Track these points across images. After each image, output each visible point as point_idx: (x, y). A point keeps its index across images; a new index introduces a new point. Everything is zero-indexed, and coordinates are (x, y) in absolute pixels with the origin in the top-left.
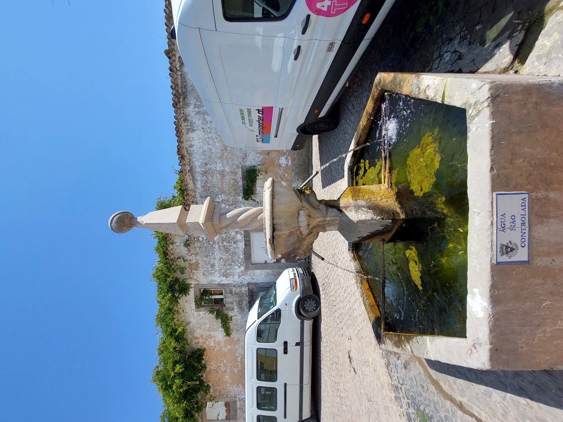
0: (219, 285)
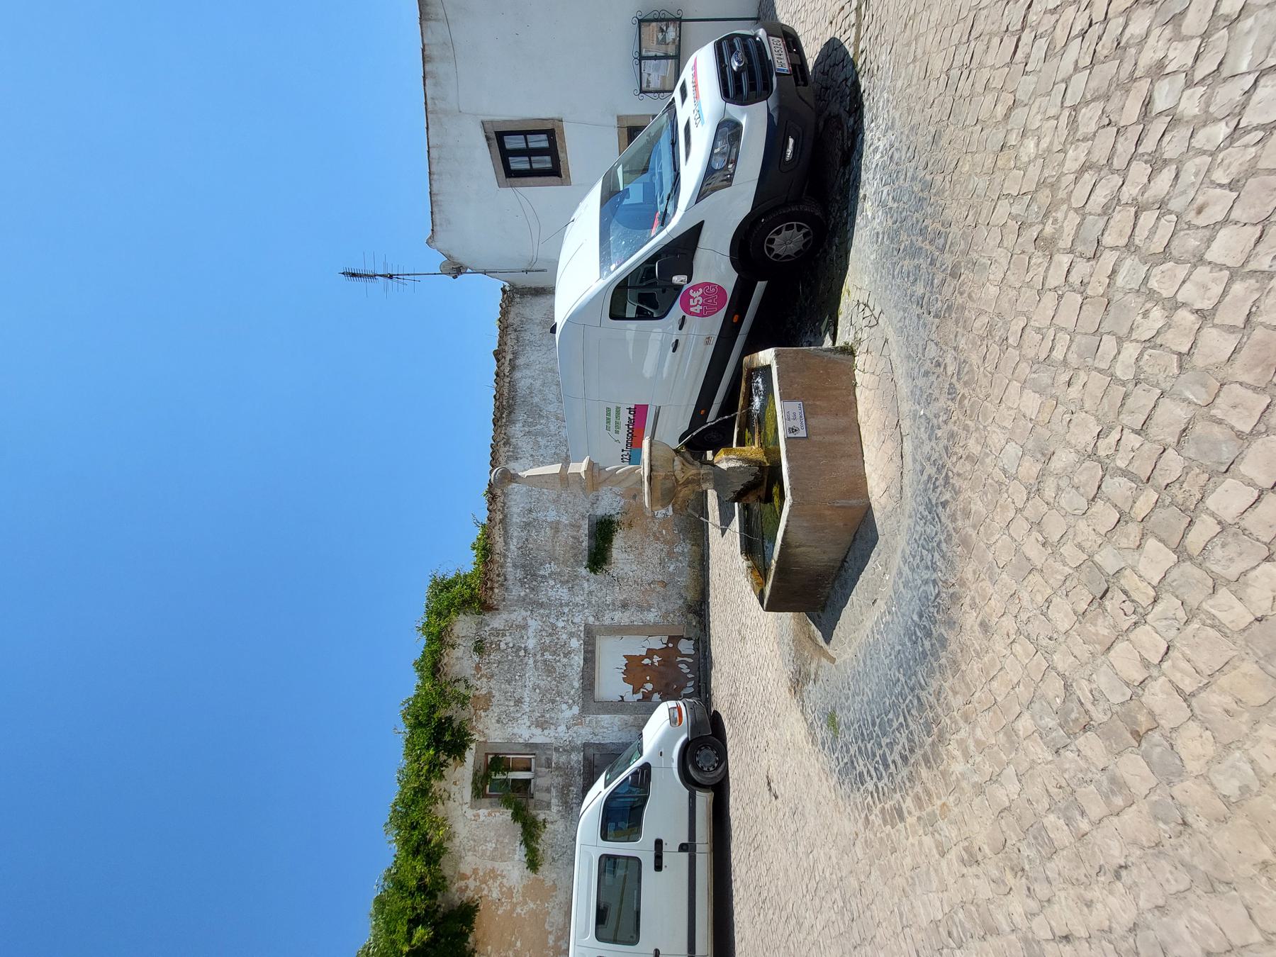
0: (527, 745)
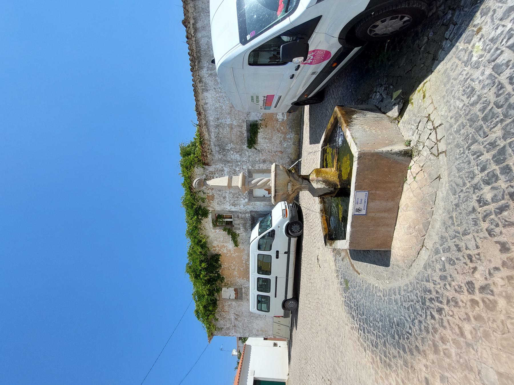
0: (229, 211)
